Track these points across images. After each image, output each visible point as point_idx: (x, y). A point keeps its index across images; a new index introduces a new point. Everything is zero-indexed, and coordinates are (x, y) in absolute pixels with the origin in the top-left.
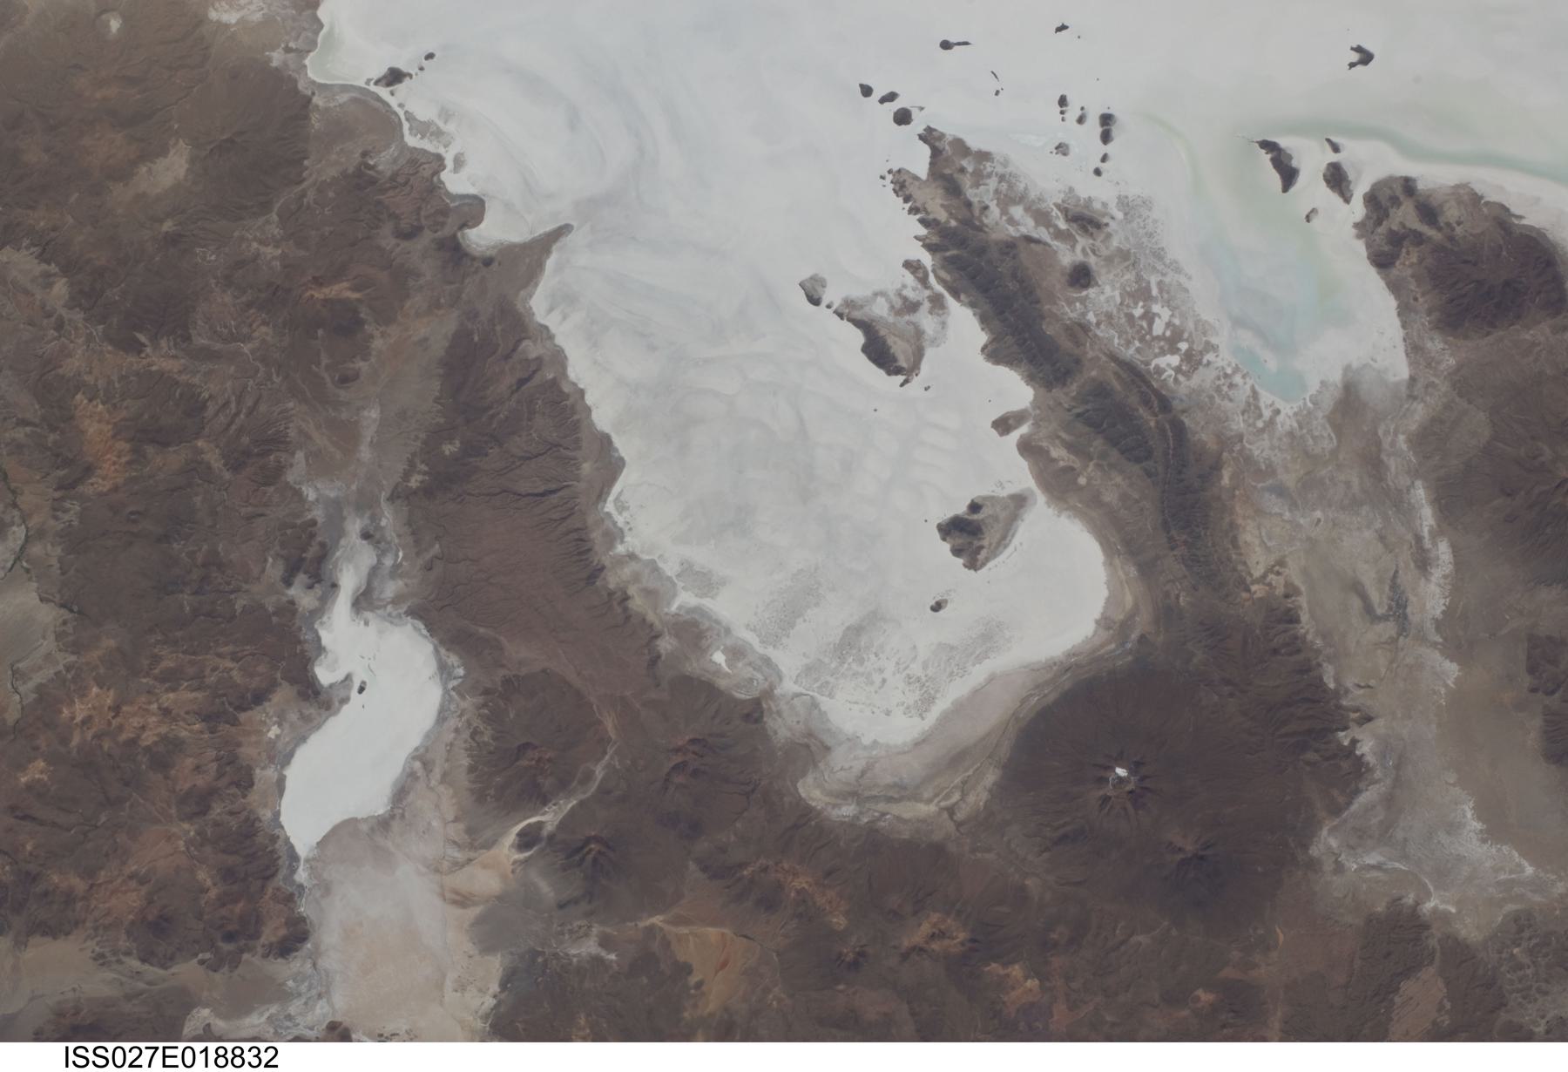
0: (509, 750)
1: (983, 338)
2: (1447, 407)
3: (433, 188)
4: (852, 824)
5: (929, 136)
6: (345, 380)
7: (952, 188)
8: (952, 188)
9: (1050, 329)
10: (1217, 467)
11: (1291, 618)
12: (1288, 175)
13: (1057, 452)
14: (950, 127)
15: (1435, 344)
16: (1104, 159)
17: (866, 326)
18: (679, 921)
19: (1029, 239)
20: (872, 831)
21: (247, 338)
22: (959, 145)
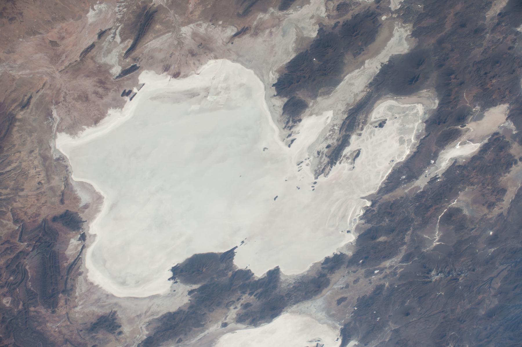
0: (449, 137)
1: (347, 148)
2: (320, 95)
3: (364, 214)
4: (438, 99)
5: (316, 178)
6: (402, 198)
7: (324, 169)
8: (324, 169)
9: (340, 143)
10: (350, 110)
11: (370, 84)
12: (292, 141)
13: (360, 126)
14: (312, 176)
15: (311, 104)
16: (306, 160)
17: (354, 160)
18: (467, 103)
19: (326, 156)
20: (438, 96)
21: (403, 211)
22: (315, 175)
